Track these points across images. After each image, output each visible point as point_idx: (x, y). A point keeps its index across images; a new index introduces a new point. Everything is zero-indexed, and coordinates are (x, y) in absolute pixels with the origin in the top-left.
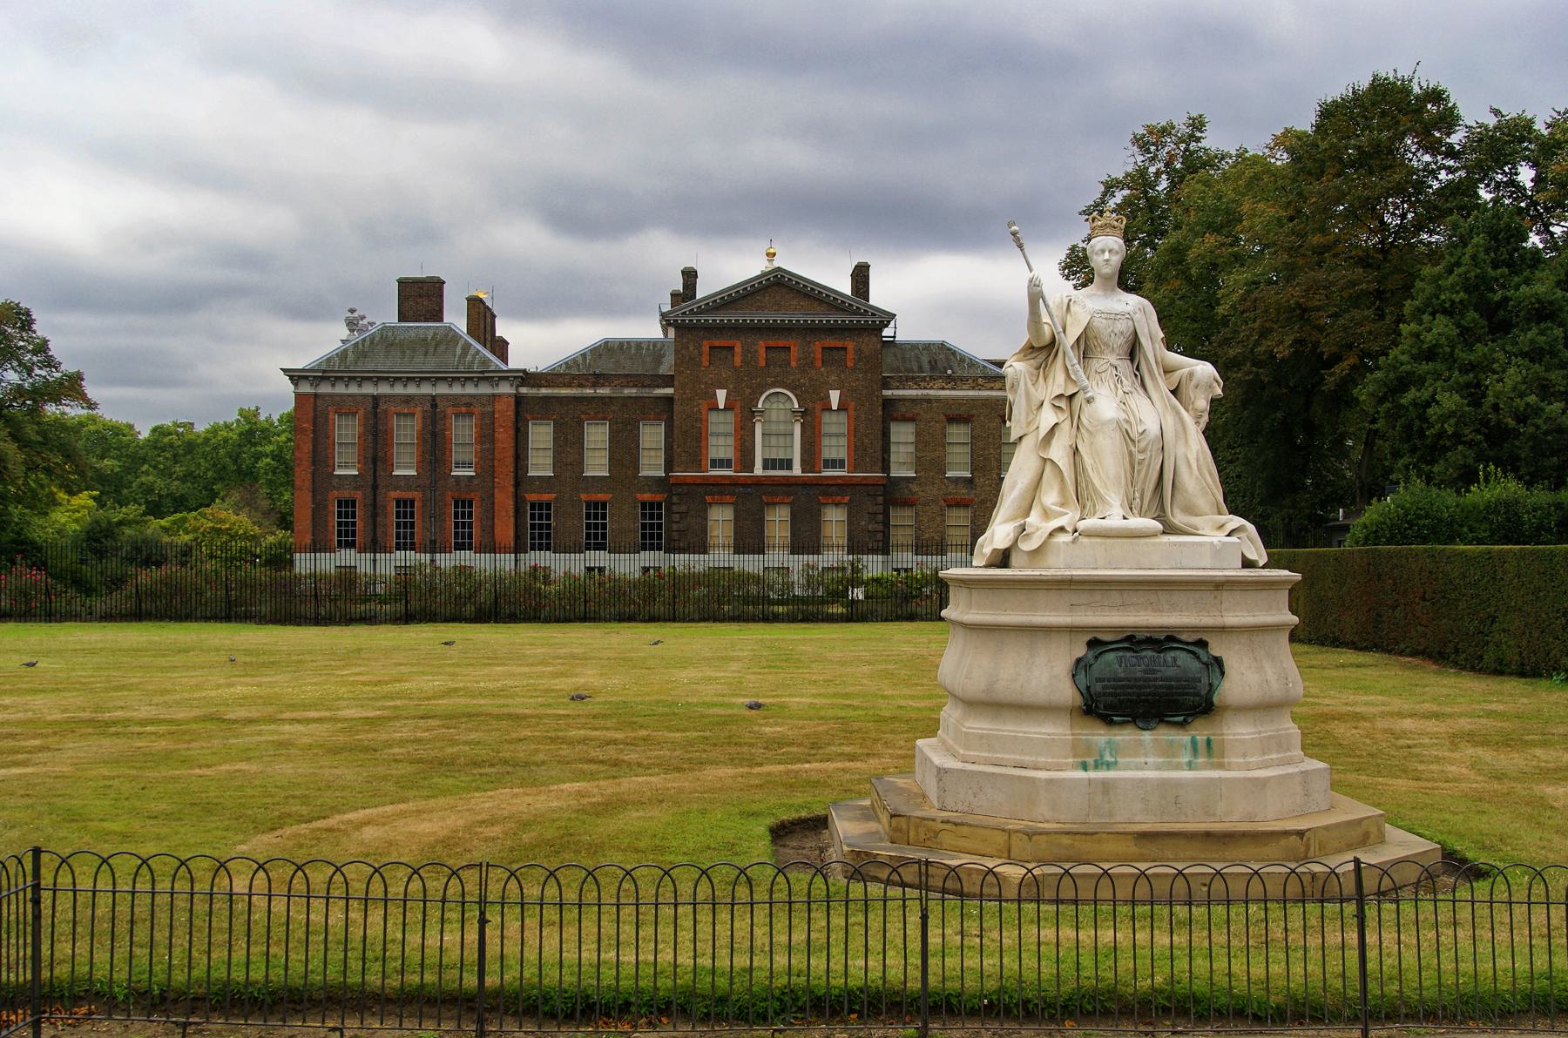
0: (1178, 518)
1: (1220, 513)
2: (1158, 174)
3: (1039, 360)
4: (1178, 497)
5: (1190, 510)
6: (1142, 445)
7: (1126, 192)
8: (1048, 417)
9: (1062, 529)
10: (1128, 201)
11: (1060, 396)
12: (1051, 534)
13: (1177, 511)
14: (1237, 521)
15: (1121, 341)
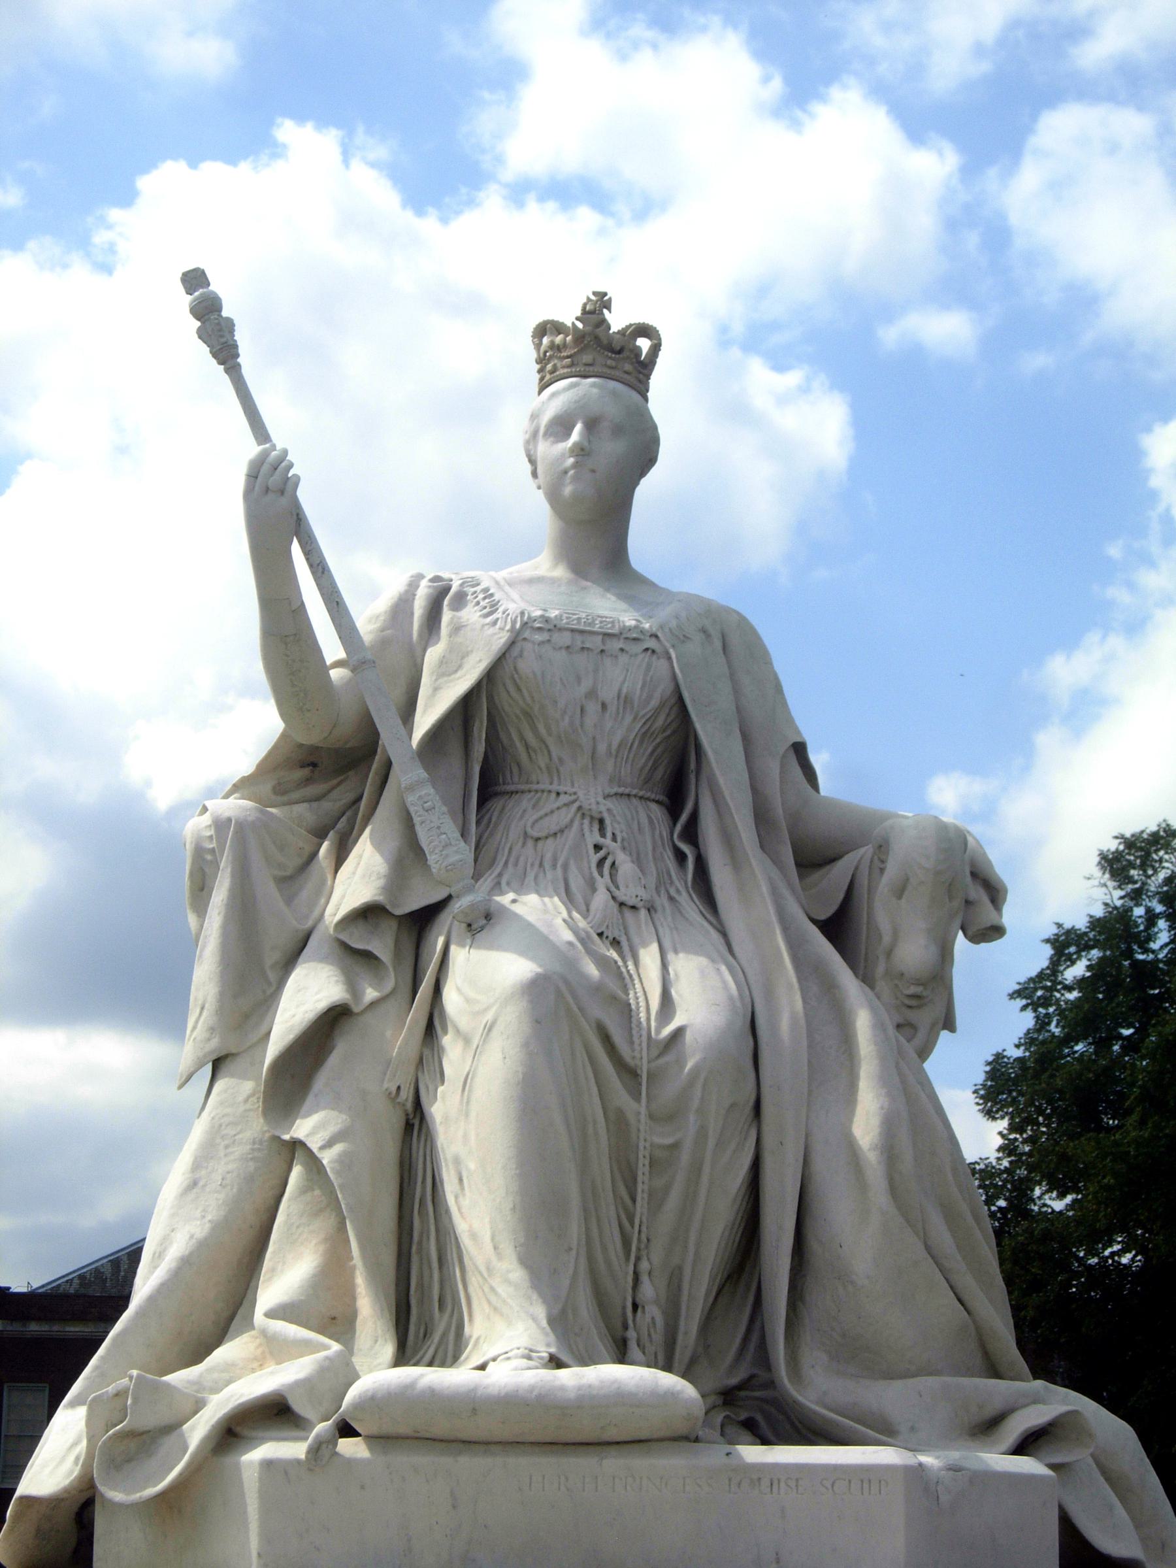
0: (816, 1386)
1: (994, 1371)
2: (1151, 918)
3: (329, 806)
4: (819, 1299)
5: (862, 1356)
6: (669, 1090)
7: (1095, 953)
8: (311, 990)
9: (275, 1413)
10: (1098, 971)
11: (368, 914)
12: (234, 1431)
13: (814, 1360)
14: (1055, 1402)
15: (619, 730)
